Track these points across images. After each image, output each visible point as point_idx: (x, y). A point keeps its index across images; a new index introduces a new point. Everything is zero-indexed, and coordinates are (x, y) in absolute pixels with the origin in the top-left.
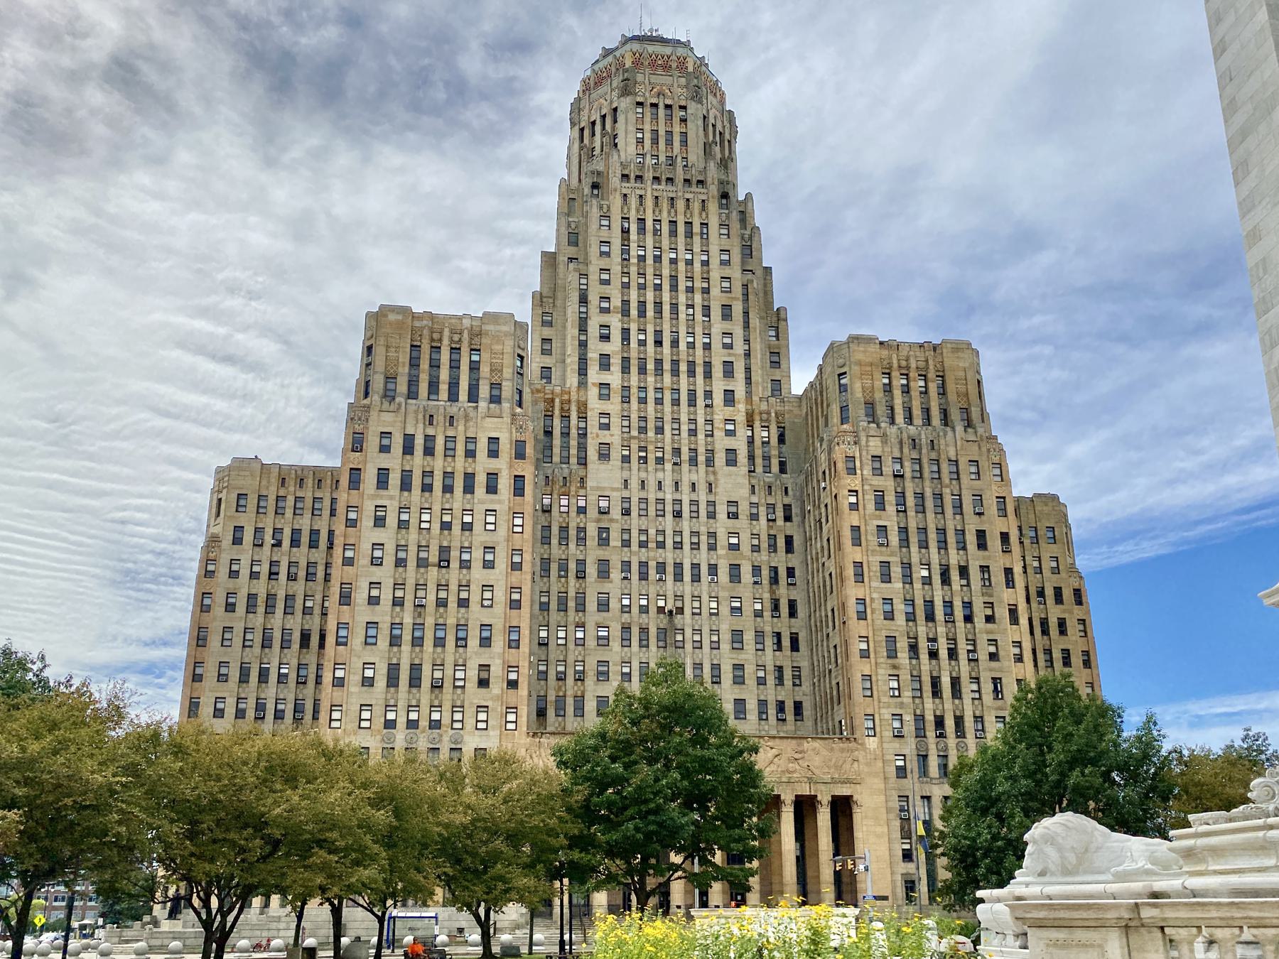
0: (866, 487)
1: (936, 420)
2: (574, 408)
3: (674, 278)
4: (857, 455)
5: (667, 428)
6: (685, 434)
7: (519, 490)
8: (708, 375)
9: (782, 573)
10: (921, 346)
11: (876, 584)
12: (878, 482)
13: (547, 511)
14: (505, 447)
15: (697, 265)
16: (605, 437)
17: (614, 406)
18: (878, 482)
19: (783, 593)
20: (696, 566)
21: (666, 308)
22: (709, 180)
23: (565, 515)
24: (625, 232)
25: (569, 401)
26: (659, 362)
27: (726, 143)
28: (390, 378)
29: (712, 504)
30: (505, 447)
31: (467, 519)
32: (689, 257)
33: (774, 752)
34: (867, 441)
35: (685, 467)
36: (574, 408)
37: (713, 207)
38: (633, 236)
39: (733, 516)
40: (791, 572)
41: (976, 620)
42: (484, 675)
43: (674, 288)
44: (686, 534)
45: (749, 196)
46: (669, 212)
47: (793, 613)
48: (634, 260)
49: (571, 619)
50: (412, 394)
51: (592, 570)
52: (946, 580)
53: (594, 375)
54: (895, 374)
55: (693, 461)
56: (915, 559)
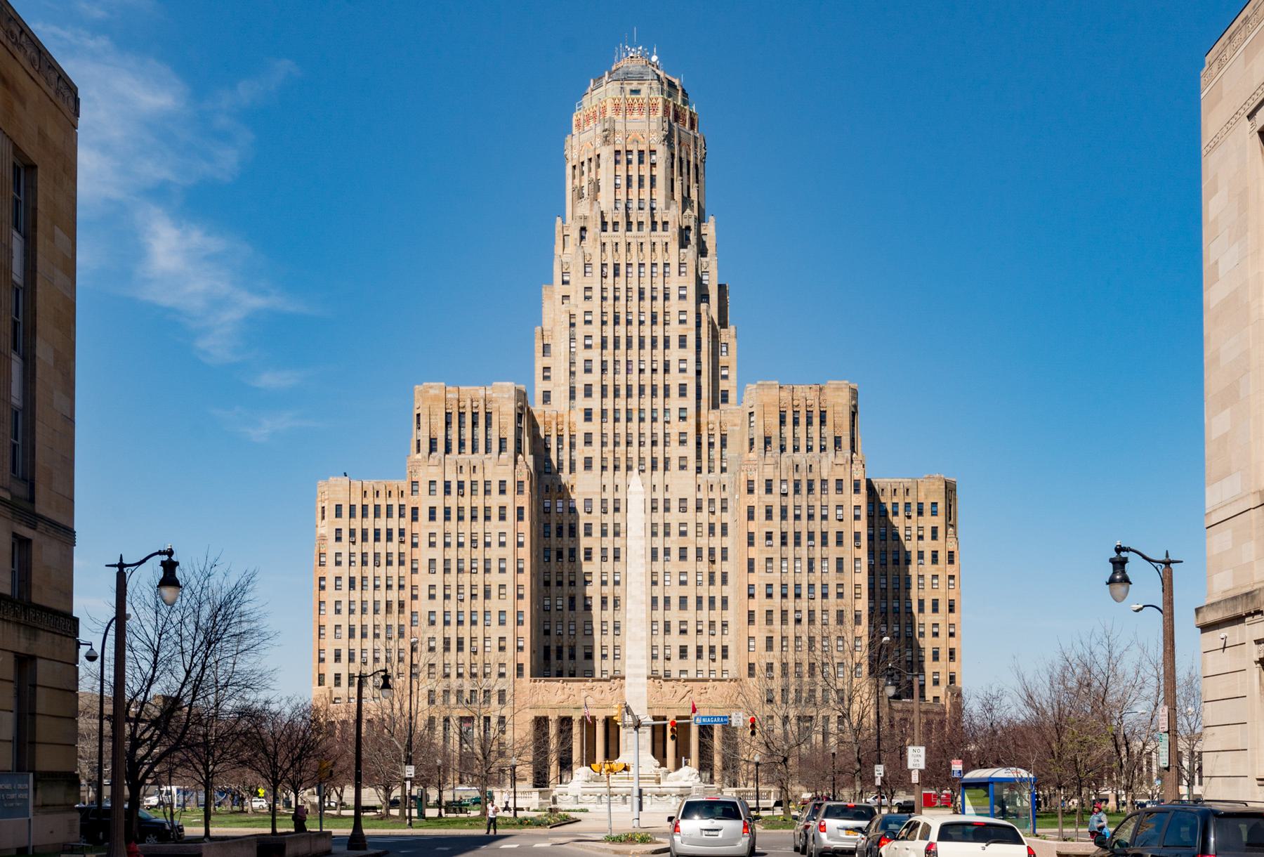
0: (761, 503)
4: (756, 479)
11: (763, 573)
13: (547, 511)
14: (510, 486)
19: (718, 568)
23: (560, 515)
25: (563, 422)
29: (666, 501)
30: (510, 486)
33: (687, 689)
34: (763, 469)
37: (674, 247)
40: (724, 550)
41: (830, 596)
47: (724, 580)
49: (566, 592)
50: (448, 450)
53: (581, 402)
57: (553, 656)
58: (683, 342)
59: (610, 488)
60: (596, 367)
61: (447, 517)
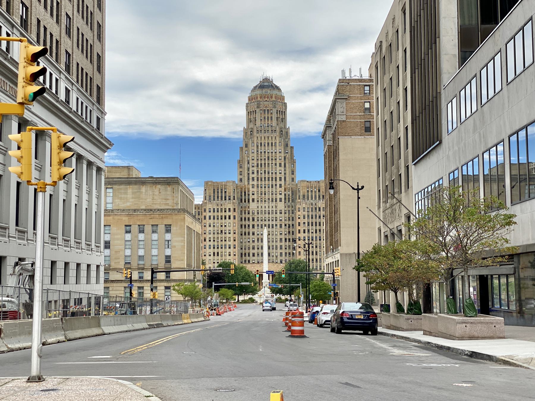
1: (317, 199)
2: (247, 190)
3: (268, 157)
5: (267, 194)
6: (271, 195)
7: (234, 218)
8: (276, 180)
9: (291, 225)
10: (316, 182)
12: (304, 213)
14: (232, 209)
15: (274, 153)
16: (253, 197)
17: (255, 189)
18: (304, 213)
19: (291, 230)
20: (273, 225)
21: (267, 165)
22: (277, 131)
24: (257, 146)
26: (265, 178)
27: (283, 114)
28: (210, 196)
30: (232, 209)
31: (225, 224)
32: (272, 151)
35: (271, 202)
36: (247, 190)
38: (259, 147)
39: (281, 213)
40: (293, 225)
42: (230, 254)
43: (268, 159)
44: (271, 218)
45: (289, 127)
46: (267, 141)
48: (259, 154)
50: (214, 200)
51: (251, 226)
52: (316, 232)
53: (251, 182)
54: (310, 188)
55: (272, 201)
56: (310, 229)
57: (243, 256)
58: (280, 165)
59: (260, 207)
60: (255, 172)
61: (214, 219)
